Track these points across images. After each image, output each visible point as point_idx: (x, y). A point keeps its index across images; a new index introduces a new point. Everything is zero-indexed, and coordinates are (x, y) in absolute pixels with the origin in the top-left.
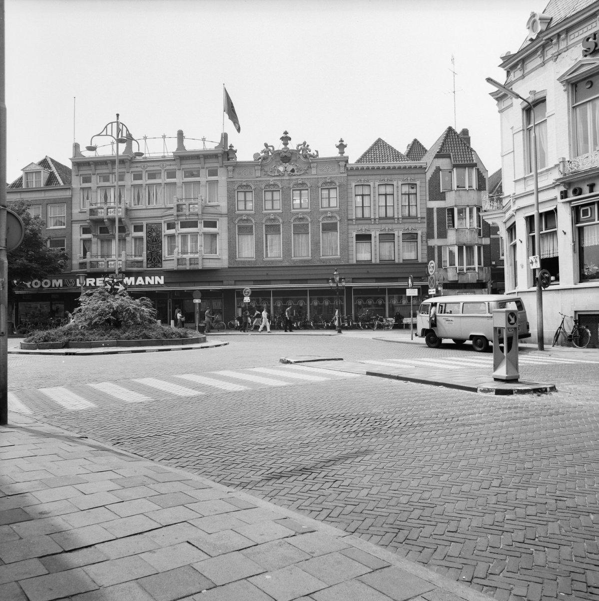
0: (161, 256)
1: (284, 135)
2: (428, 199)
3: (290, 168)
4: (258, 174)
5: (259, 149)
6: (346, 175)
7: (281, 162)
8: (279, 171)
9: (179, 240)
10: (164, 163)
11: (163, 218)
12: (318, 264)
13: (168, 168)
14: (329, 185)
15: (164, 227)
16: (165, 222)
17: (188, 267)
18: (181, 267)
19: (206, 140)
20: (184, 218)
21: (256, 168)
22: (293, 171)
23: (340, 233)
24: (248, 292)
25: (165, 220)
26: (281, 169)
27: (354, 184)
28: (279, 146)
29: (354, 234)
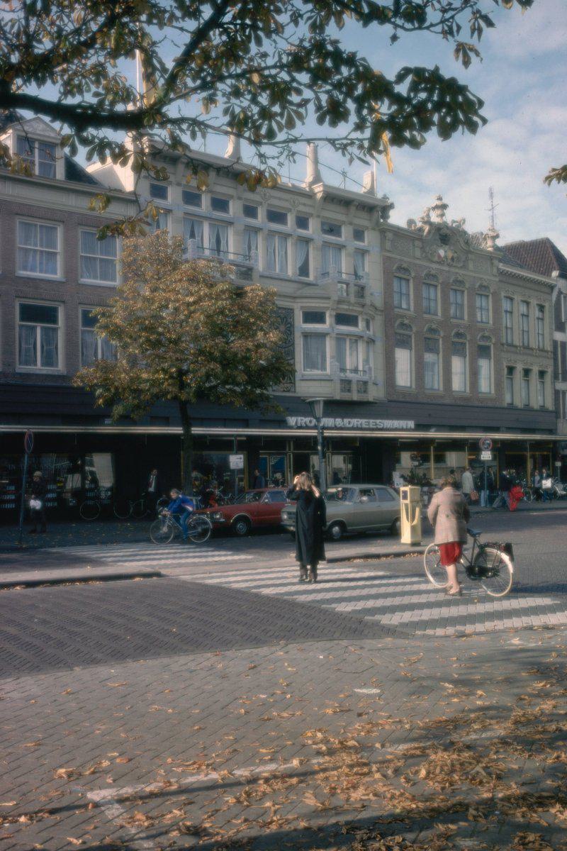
0: (293, 372)
1: (439, 203)
2: (554, 328)
3: (450, 254)
4: (418, 253)
5: (418, 217)
6: (497, 280)
7: (440, 242)
8: (439, 256)
9: (329, 346)
10: (296, 197)
11: (298, 300)
12: (476, 403)
13: (301, 208)
14: (482, 291)
15: (298, 317)
16: (302, 307)
17: (355, 396)
18: (346, 396)
19: (348, 175)
20: (346, 307)
21: (417, 243)
22: (452, 259)
23: (495, 361)
24: (489, 444)
25: (304, 305)
26: (442, 252)
27: (503, 294)
28: (435, 218)
29: (505, 364)
